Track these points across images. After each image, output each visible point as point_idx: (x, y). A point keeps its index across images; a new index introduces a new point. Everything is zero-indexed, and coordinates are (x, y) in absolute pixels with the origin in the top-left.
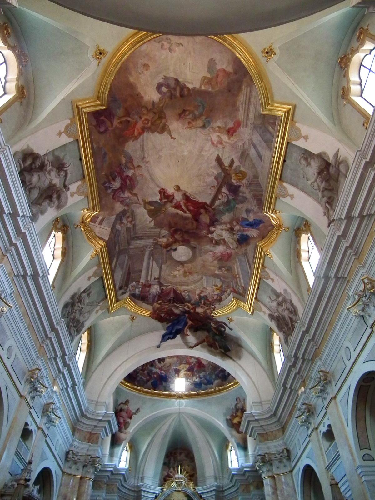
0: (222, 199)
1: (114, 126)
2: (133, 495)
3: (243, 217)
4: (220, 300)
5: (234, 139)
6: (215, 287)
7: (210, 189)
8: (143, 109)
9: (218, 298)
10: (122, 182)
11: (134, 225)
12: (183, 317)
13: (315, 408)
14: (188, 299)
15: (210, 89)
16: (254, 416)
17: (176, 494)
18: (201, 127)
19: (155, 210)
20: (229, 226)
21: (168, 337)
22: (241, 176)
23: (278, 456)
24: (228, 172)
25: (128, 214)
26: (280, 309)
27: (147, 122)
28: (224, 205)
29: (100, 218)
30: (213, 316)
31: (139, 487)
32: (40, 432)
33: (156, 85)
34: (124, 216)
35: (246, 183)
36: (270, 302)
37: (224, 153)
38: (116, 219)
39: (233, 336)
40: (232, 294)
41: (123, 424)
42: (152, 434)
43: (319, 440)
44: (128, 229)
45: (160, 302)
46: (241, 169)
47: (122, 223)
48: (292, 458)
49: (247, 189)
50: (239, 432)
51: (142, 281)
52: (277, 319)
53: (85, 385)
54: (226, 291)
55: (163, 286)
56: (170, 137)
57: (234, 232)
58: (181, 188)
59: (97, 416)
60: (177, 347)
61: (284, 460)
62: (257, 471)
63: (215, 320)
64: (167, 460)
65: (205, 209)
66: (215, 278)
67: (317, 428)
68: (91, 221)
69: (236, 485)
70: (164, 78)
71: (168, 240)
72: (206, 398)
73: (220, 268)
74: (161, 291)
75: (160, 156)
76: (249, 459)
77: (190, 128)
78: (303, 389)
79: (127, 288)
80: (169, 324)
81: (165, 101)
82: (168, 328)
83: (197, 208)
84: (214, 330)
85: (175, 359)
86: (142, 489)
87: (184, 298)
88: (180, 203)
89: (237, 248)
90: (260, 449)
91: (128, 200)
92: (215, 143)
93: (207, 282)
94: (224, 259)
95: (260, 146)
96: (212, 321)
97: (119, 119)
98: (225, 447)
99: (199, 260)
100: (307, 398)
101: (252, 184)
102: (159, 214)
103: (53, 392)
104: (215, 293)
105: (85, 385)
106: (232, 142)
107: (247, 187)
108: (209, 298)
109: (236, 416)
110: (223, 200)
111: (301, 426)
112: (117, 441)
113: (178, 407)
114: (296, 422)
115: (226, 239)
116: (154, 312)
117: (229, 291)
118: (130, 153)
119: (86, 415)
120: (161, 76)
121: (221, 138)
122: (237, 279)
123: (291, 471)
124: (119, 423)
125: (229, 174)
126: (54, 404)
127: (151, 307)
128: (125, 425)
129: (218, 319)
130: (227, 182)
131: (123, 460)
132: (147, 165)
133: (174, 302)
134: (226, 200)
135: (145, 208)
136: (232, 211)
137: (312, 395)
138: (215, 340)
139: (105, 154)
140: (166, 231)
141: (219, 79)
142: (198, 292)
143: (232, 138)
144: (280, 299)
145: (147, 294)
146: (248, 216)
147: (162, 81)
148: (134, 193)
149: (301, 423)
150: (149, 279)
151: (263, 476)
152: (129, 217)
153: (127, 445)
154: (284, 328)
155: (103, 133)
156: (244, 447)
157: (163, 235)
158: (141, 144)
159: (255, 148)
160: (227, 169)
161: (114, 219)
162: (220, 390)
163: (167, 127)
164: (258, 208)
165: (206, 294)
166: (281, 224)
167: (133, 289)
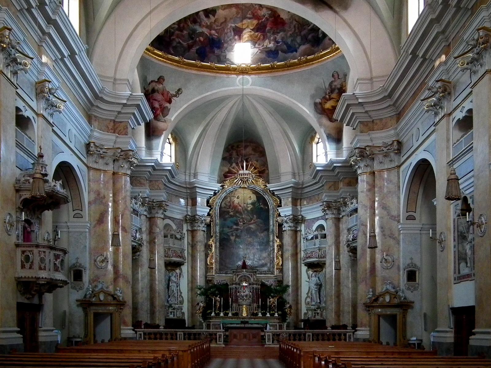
2: (185, 191)
13: (455, 87)
16: (357, 99)
17: (240, 190)
23: (384, 149)
31: (191, 183)
32: (41, 119)
41: (160, 110)
42: (204, 123)
43: (448, 130)
48: (404, 151)
50: (331, 120)
53: (89, 53)
59: (119, 98)
61: (392, 154)
62: (351, 166)
64: (227, 155)
67: (450, 114)
69: (321, 182)
72: (285, 73)
76: (342, 153)
78: (443, 58)
85: (234, 10)
86: (196, 185)
90: (359, 141)
98: (309, 139)
100: (448, 71)
103: (42, 64)
105: (89, 53)
109: (330, 99)
111: (427, 111)
112: (154, 132)
113: (240, 87)
114: (421, 106)
119: (102, 98)
123: (399, 167)
124: (153, 109)
126: (50, 82)
128: (162, 111)
131: (165, 153)
137: (456, 66)
149: (428, 107)
151: (359, 172)
153: (170, 137)
156: (336, 138)
162: (307, 61)
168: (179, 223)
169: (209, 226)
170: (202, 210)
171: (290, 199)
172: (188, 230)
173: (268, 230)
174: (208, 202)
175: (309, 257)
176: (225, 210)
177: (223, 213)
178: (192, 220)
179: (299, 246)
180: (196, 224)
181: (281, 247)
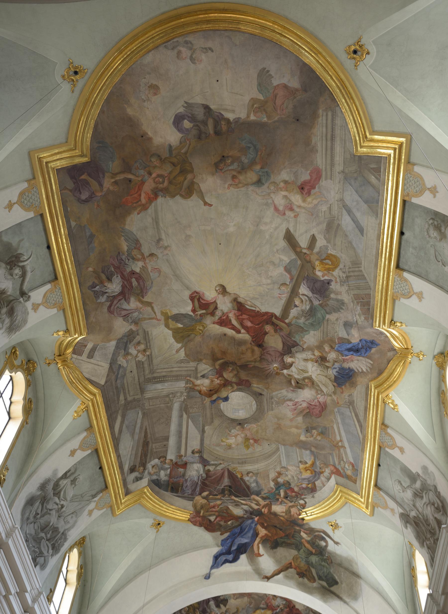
0: (301, 305)
1: (105, 189)
3: (340, 336)
4: (313, 490)
5: (313, 200)
6: (301, 466)
7: (279, 288)
8: (153, 160)
9: (310, 486)
10: (123, 282)
11: (150, 358)
12: (250, 521)
14: (256, 489)
15: (265, 119)
18: (254, 184)
19: (185, 328)
20: (317, 353)
21: (223, 558)
22: (330, 263)
24: (308, 258)
25: (138, 338)
27: (161, 180)
28: (305, 317)
29: (90, 346)
30: (303, 519)
33: (173, 117)
34: (130, 342)
35: (339, 277)
36: (401, 491)
37: (298, 225)
38: (117, 347)
39: (340, 556)
40: (333, 476)
44: (139, 364)
45: (205, 494)
46: (329, 252)
47: (128, 354)
49: (343, 285)
51: (171, 456)
52: (415, 522)
54: (322, 473)
55: (209, 465)
56: (202, 203)
57: (327, 364)
58: (228, 290)
60: (241, 576)
63: (306, 527)
65: (273, 324)
66: (300, 448)
68: (74, 352)
70: (185, 105)
71: (212, 381)
73: (307, 431)
74: (207, 474)
75: (188, 237)
77: (236, 186)
79: (145, 469)
80: (226, 535)
81: (190, 144)
82: (223, 542)
83: (258, 324)
84: (307, 545)
85: (246, 599)
87: (248, 487)
88: (228, 316)
89: (334, 393)
91: (136, 314)
92: (281, 208)
93: (288, 456)
94: (314, 413)
95: (358, 209)
96: (303, 528)
97: (112, 178)
99: (270, 416)
101: (350, 276)
102: (193, 335)
104: (303, 477)
106: (310, 206)
107: (342, 283)
108: (292, 486)
110: (304, 308)
115: (314, 377)
116: (197, 513)
117: (327, 471)
118: (135, 233)
120: (180, 103)
121: (290, 201)
122: (339, 451)
125: (310, 262)
127: (189, 504)
129: (314, 525)
130: (307, 275)
132: (166, 252)
133: (231, 494)
134: (308, 307)
135: (167, 326)
136: (320, 327)
138: (309, 564)
139: (92, 236)
140: (208, 367)
141: (279, 102)
142: (272, 475)
143: (309, 199)
144: (418, 485)
145: (182, 480)
146: (348, 335)
147: (182, 110)
148: (147, 302)
150: (183, 452)
152: (139, 343)
154: (429, 540)
155: (86, 201)
157: (202, 374)
158: (154, 218)
159: (349, 215)
160: (306, 253)
161: (114, 348)
163: (196, 187)
164: (366, 318)
165: (287, 479)
166: (410, 347)
167: (154, 470)
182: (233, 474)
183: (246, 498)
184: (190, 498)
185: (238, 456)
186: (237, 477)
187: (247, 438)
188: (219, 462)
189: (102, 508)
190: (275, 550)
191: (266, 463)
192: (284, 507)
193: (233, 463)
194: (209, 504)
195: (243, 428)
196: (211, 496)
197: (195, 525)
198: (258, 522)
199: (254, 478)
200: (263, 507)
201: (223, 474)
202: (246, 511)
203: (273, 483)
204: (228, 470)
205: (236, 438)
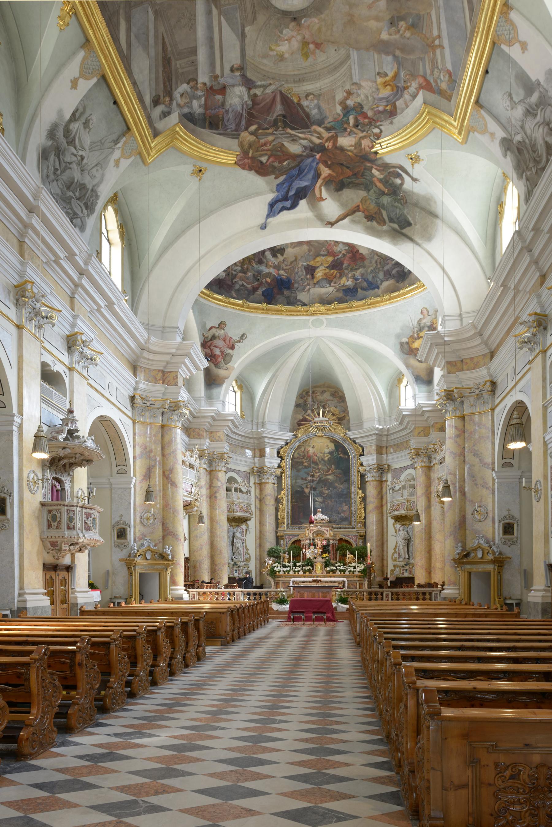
12: (310, 160)
14: (318, 117)
17: (315, 439)
21: (280, 205)
26: (530, 124)
31: (257, 433)
45: (253, 128)
55: (256, 87)
74: (253, 101)
87: (308, 115)
112: (215, 380)
116: (245, 153)
133: (286, 125)
142: (340, 96)
145: (221, 111)
150: (218, 71)
156: (425, 379)
168: (247, 476)
169: (279, 478)
170: (271, 461)
171: (374, 447)
172: (255, 483)
173: (348, 480)
174: (278, 453)
175: (397, 510)
176: (298, 460)
177: (296, 464)
178: (260, 472)
179: (385, 497)
180: (265, 477)
181: (364, 499)
182: (288, 97)
183: (304, 130)
184: (235, 135)
185: (294, 71)
186: (292, 102)
187: (306, 42)
188: (268, 82)
189: (130, 157)
190: (340, 192)
191: (332, 78)
192: (354, 139)
193: (287, 82)
194: (259, 142)
195: (299, 25)
196: (260, 131)
197: (244, 169)
198: (320, 160)
199: (316, 102)
200: (326, 141)
201: (274, 99)
202: (305, 147)
203: (341, 108)
204: (281, 92)
205: (289, 42)
